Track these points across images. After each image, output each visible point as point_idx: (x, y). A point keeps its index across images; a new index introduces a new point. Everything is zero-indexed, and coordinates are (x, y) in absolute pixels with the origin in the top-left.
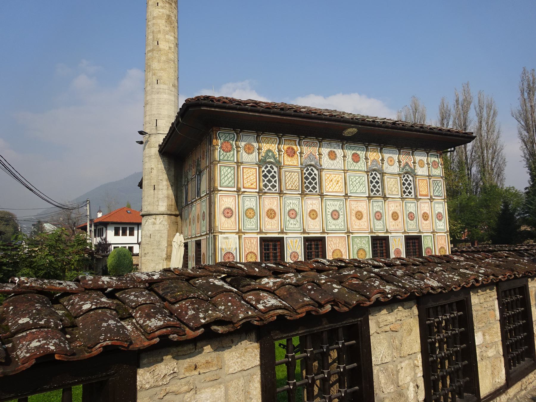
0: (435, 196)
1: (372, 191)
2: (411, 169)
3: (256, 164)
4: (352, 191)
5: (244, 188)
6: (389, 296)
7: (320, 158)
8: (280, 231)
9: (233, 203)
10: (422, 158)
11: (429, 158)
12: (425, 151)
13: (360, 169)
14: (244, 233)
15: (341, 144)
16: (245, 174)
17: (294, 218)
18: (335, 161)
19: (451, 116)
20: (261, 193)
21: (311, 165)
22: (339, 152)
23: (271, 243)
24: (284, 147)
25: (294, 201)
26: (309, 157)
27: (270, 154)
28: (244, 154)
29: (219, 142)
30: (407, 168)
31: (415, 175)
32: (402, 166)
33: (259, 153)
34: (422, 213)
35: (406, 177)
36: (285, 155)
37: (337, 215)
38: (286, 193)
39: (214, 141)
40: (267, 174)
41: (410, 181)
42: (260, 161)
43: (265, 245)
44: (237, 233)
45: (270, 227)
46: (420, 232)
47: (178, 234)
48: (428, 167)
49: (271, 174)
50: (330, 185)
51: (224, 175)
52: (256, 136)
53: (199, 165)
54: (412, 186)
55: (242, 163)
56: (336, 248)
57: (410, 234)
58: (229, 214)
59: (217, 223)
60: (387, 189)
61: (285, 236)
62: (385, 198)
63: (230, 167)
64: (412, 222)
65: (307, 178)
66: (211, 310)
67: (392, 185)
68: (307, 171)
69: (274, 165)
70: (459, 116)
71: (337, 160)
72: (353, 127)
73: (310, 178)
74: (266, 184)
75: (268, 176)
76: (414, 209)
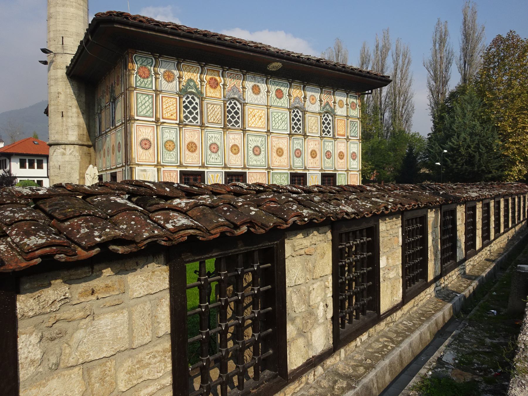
0: (351, 136)
1: (293, 128)
3: (177, 94)
4: (274, 128)
5: (163, 118)
6: (306, 219)
8: (200, 165)
9: (151, 134)
10: (342, 98)
11: (349, 99)
12: (345, 91)
13: (283, 105)
14: (163, 166)
15: (265, 79)
16: (164, 104)
17: (216, 152)
18: (259, 96)
19: (371, 61)
20: (181, 124)
21: (234, 99)
22: (263, 87)
23: (192, 177)
24: (206, 77)
25: (215, 135)
26: (232, 89)
27: (192, 84)
28: (164, 82)
29: (136, 67)
31: (334, 115)
32: (323, 105)
33: (180, 82)
35: (326, 116)
36: (208, 86)
37: (259, 151)
38: (207, 127)
39: (130, 64)
40: (188, 105)
41: (330, 120)
42: (180, 90)
43: (185, 179)
44: (155, 166)
45: (191, 161)
46: (335, 170)
47: (91, 166)
48: (347, 108)
49: (193, 106)
50: (253, 121)
51: (140, 103)
52: (176, 62)
53: (113, 91)
54: (331, 125)
55: (161, 91)
57: (326, 172)
58: (147, 146)
59: (134, 155)
60: (307, 127)
61: (206, 170)
62: (305, 136)
63: (148, 95)
65: (229, 112)
66: (109, 228)
67: (313, 124)
68: (229, 104)
69: (196, 96)
70: (378, 62)
71: (261, 95)
72: (278, 62)
73: (233, 112)
74: (187, 115)
75: (189, 108)
76: (332, 148)
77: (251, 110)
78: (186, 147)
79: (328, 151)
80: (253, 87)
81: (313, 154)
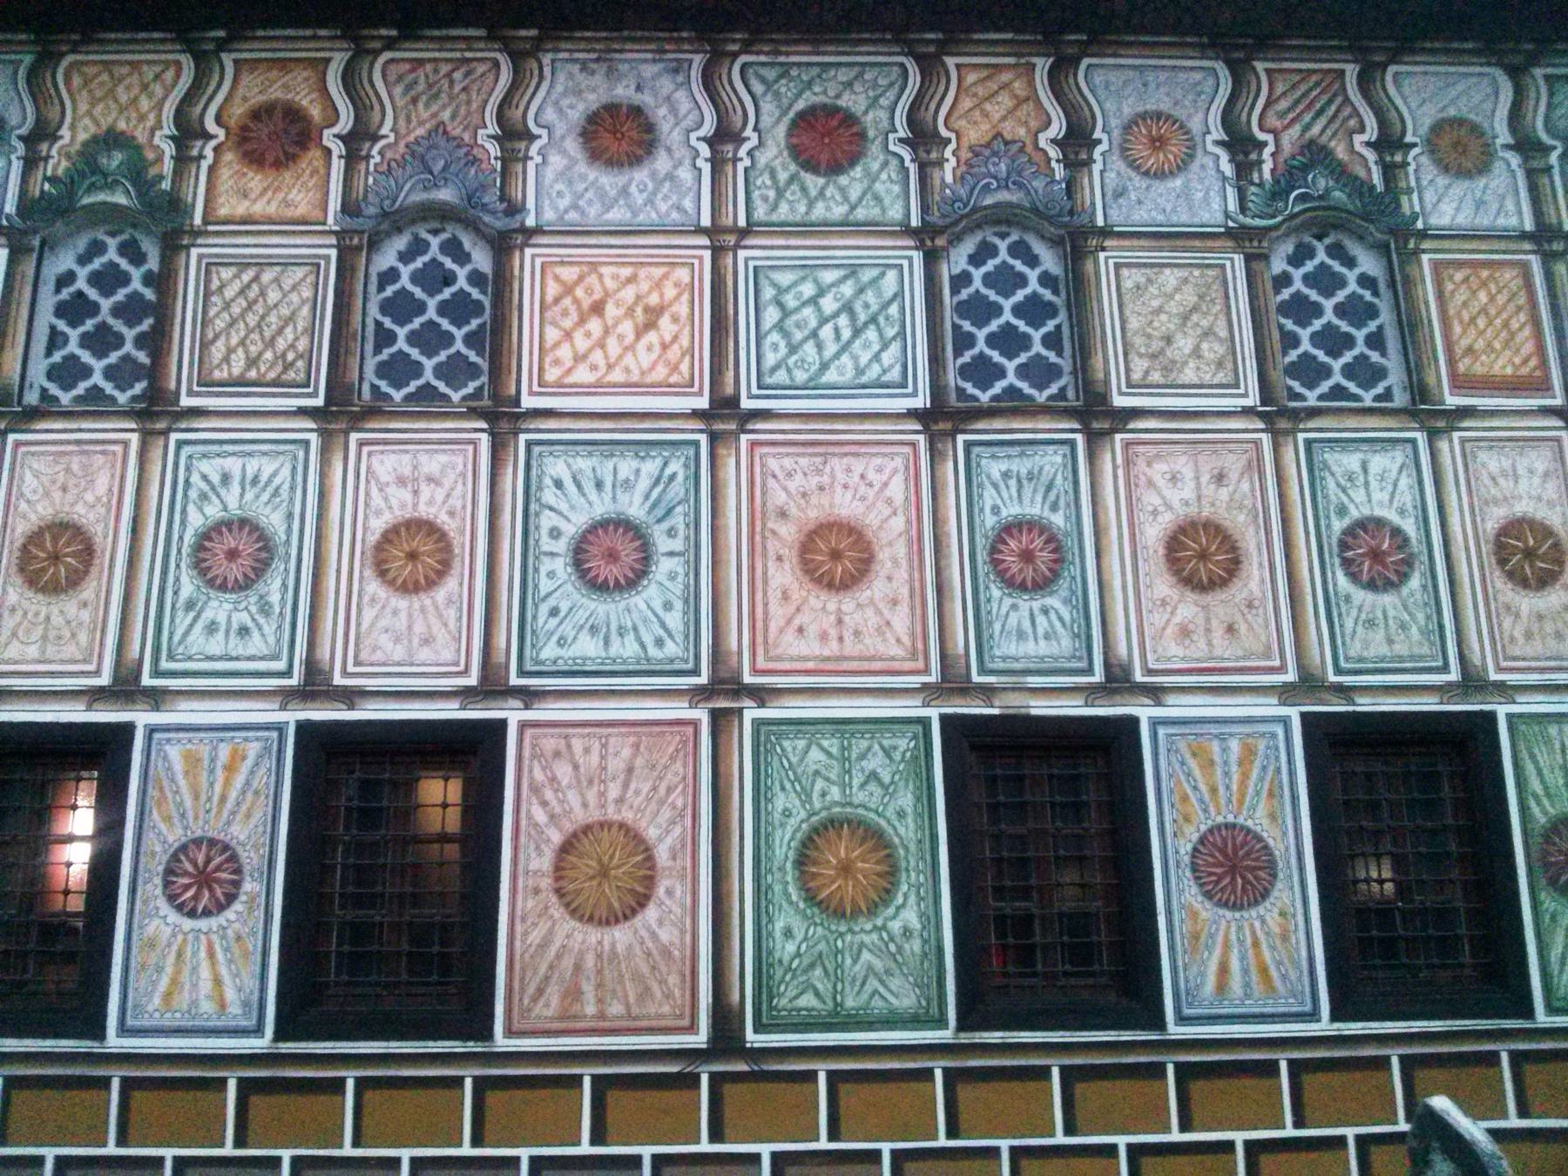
2: (1361, 188)
4: (781, 377)
7: (508, 159)
8: (105, 680)
13: (860, 214)
15: (698, 60)
17: (244, 585)
18: (641, 175)
21: (440, 214)
25: (252, 466)
26: (418, 156)
30: (1321, 182)
31: (1399, 238)
35: (1321, 256)
36: (229, 156)
37: (628, 552)
42: (26, 206)
46: (1472, 682)
54: (1386, 317)
56: (595, 815)
57: (1365, 705)
60: (1114, 347)
62: (1096, 415)
64: (1388, 599)
67: (1172, 321)
71: (662, 163)
74: (73, 358)
76: (1406, 496)
77: (569, 274)
79: (1369, 525)
80: (593, 119)
81: (1202, 556)
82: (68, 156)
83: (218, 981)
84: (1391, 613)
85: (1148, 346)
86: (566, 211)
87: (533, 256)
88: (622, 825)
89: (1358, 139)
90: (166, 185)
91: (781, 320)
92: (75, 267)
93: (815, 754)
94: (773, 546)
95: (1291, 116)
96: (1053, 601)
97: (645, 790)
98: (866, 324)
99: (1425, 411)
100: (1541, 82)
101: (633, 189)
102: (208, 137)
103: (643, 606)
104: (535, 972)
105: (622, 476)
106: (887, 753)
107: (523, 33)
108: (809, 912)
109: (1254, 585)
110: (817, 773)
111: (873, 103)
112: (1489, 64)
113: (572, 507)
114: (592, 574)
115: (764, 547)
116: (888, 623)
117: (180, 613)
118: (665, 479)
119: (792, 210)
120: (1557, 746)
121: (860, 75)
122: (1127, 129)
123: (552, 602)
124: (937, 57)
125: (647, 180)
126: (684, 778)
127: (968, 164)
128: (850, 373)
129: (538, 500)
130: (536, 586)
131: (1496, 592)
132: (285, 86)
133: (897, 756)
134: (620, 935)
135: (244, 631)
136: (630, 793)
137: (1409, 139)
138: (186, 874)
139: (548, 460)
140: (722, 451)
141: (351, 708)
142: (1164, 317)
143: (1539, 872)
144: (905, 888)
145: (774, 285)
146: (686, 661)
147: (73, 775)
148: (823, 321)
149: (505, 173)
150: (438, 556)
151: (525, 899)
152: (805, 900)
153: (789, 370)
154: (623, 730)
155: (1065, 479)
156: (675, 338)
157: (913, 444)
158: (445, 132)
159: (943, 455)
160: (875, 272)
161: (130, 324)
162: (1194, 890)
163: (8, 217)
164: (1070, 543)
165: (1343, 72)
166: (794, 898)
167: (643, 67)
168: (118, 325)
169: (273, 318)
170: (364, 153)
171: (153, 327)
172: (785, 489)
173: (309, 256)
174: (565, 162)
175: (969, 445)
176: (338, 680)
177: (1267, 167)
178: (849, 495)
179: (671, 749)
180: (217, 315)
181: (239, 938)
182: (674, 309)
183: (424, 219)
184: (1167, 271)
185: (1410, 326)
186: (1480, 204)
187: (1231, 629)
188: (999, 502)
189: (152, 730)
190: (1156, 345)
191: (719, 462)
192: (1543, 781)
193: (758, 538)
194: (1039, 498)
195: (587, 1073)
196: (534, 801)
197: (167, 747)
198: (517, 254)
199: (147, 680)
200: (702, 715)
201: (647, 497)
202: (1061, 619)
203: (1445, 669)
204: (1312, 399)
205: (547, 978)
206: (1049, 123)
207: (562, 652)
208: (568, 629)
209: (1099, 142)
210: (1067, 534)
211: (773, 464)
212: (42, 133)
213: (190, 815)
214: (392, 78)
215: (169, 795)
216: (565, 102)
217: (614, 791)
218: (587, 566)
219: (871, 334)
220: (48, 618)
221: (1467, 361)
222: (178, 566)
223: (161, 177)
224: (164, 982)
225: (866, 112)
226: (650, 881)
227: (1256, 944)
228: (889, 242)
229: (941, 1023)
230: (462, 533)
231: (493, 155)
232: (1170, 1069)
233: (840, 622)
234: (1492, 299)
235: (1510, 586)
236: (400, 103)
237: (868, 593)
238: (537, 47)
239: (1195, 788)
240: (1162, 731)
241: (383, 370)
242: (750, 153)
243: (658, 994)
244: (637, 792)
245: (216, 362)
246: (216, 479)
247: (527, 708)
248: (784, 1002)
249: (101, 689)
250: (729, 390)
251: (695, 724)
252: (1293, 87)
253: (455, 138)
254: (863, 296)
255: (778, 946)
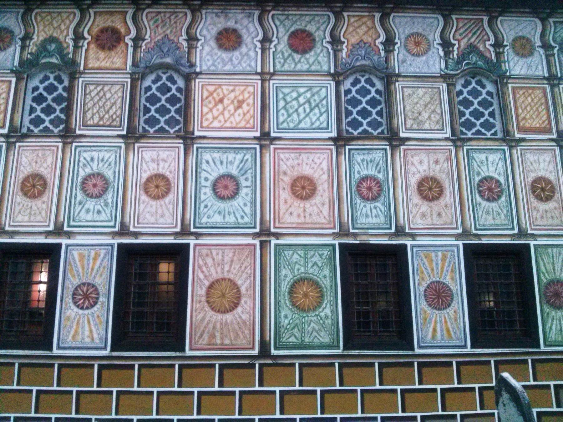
2: (488, 61)
4: (285, 125)
7: (190, 47)
8: (51, 228)
13: (313, 68)
15: (257, 13)
18: (236, 53)
21: (166, 67)
25: (101, 155)
26: (159, 46)
31: (501, 79)
34: (530, 179)
35: (474, 84)
36: (92, 46)
42: (22, 63)
46: (522, 233)
54: (495, 106)
56: (220, 276)
57: (485, 241)
60: (401, 116)
62: (394, 140)
64: (494, 205)
67: (421, 107)
71: (244, 49)
74: (38, 116)
77: (211, 88)
78: (18, 186)
81: (430, 189)
82: (36, 46)
83: (91, 331)
84: (495, 209)
85: (412, 115)
86: (210, 66)
87: (199, 82)
88: (229, 280)
89: (487, 43)
90: (70, 56)
91: (285, 106)
92: (39, 84)
93: (296, 256)
94: (281, 184)
95: (464, 35)
96: (378, 204)
97: (237, 268)
98: (315, 107)
99: (509, 140)
100: (552, 24)
101: (234, 59)
102: (85, 39)
103: (236, 205)
104: (199, 329)
105: (230, 159)
106: (320, 256)
107: (196, 3)
108: (293, 310)
109: (448, 199)
110: (296, 262)
111: (318, 29)
112: (533, 17)
113: (212, 170)
114: (219, 194)
115: (279, 185)
116: (321, 212)
117: (77, 205)
118: (244, 161)
119: (290, 67)
120: (551, 256)
121: (313, 19)
122: (407, 39)
123: (205, 203)
124: (341, 12)
125: (239, 56)
126: (251, 264)
127: (351, 51)
128: (309, 125)
129: (201, 168)
130: (200, 197)
131: (531, 202)
132: (113, 22)
133: (324, 257)
134: (228, 317)
135: (99, 212)
136: (232, 268)
137: (505, 43)
138: (80, 295)
139: (204, 154)
140: (264, 151)
141: (137, 238)
142: (418, 105)
143: (543, 298)
144: (326, 301)
145: (283, 93)
146: (252, 224)
147: (39, 261)
148: (300, 106)
149: (189, 53)
150: (166, 187)
151: (196, 304)
152: (292, 305)
153: (288, 123)
154: (230, 247)
155: (383, 162)
156: (248, 112)
157: (331, 150)
158: (168, 37)
159: (341, 153)
160: (318, 89)
161: (59, 104)
162: (425, 303)
163: (15, 67)
164: (384, 184)
165: (482, 19)
166: (288, 305)
167: (237, 15)
168: (54, 105)
169: (108, 103)
170: (140, 45)
171: (67, 106)
172: (286, 165)
173: (122, 82)
174: (210, 49)
175: (350, 150)
176: (132, 229)
177: (455, 53)
178: (308, 167)
179: (246, 254)
180: (89, 102)
181: (98, 317)
182: (248, 101)
183: (160, 69)
184: (420, 89)
185: (504, 109)
186: (529, 67)
187: (439, 214)
188: (360, 170)
189: (67, 246)
190: (416, 115)
191: (263, 155)
192: (545, 268)
193: (276, 182)
194: (374, 169)
195: (217, 363)
196: (199, 271)
197: (73, 252)
198: (193, 81)
199: (66, 229)
200: (257, 242)
201: (238, 167)
202: (381, 210)
203: (513, 229)
204: (469, 135)
205: (204, 331)
206: (379, 36)
207: (209, 220)
208: (211, 212)
209: (397, 43)
210: (383, 181)
211: (282, 156)
212: (27, 37)
213: (81, 275)
214: (149, 18)
215: (74, 268)
216: (210, 28)
217: (227, 268)
218: (217, 191)
219: (316, 111)
220: (31, 207)
221: (523, 122)
222: (76, 189)
223: (69, 53)
224: (72, 332)
225: (315, 32)
226: (239, 298)
227: (446, 322)
228: (323, 78)
229: (338, 347)
230: (174, 179)
231: (185, 46)
232: (416, 364)
233: (305, 211)
234: (532, 100)
235: (536, 200)
236: (152, 27)
237: (314, 201)
238: (200, 7)
239: (426, 269)
240: (415, 249)
241: (146, 122)
242: (275, 46)
243: (242, 337)
244: (235, 268)
245: (89, 118)
246: (89, 159)
247: (197, 239)
248: (284, 339)
249: (50, 232)
250: (267, 130)
251: (254, 245)
252: (466, 24)
253: (171, 40)
254: (314, 97)
255: (283, 321)
